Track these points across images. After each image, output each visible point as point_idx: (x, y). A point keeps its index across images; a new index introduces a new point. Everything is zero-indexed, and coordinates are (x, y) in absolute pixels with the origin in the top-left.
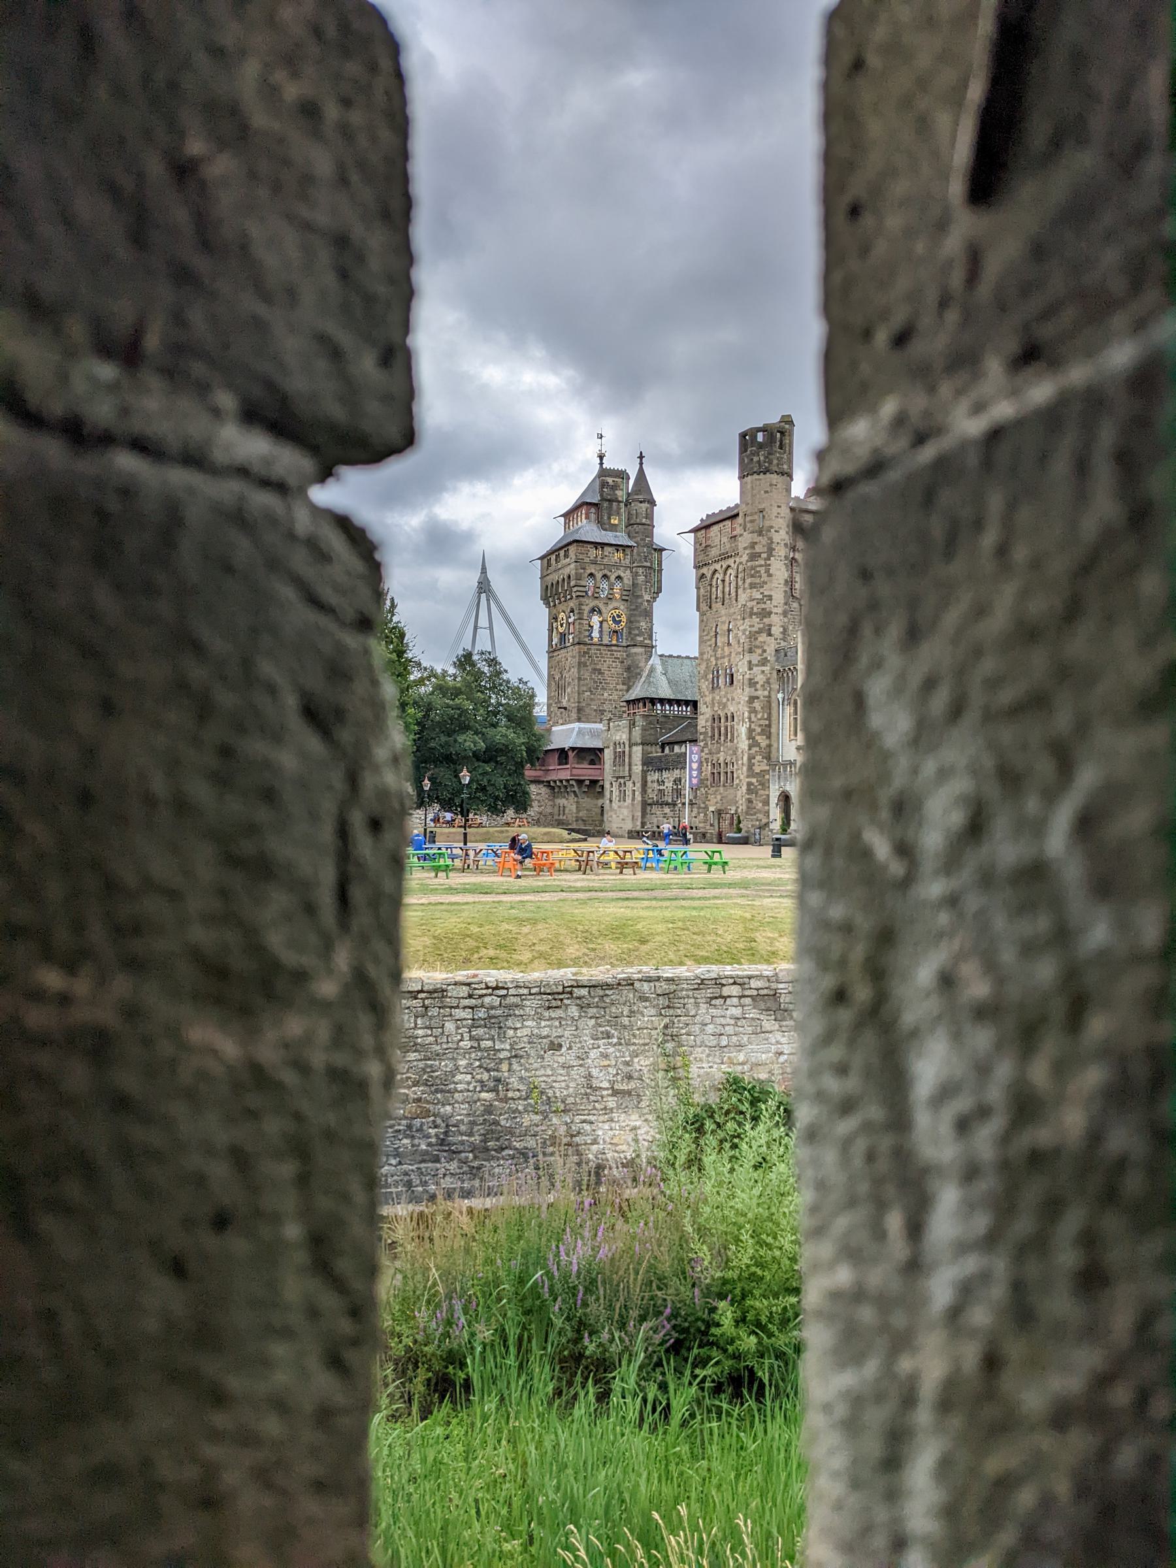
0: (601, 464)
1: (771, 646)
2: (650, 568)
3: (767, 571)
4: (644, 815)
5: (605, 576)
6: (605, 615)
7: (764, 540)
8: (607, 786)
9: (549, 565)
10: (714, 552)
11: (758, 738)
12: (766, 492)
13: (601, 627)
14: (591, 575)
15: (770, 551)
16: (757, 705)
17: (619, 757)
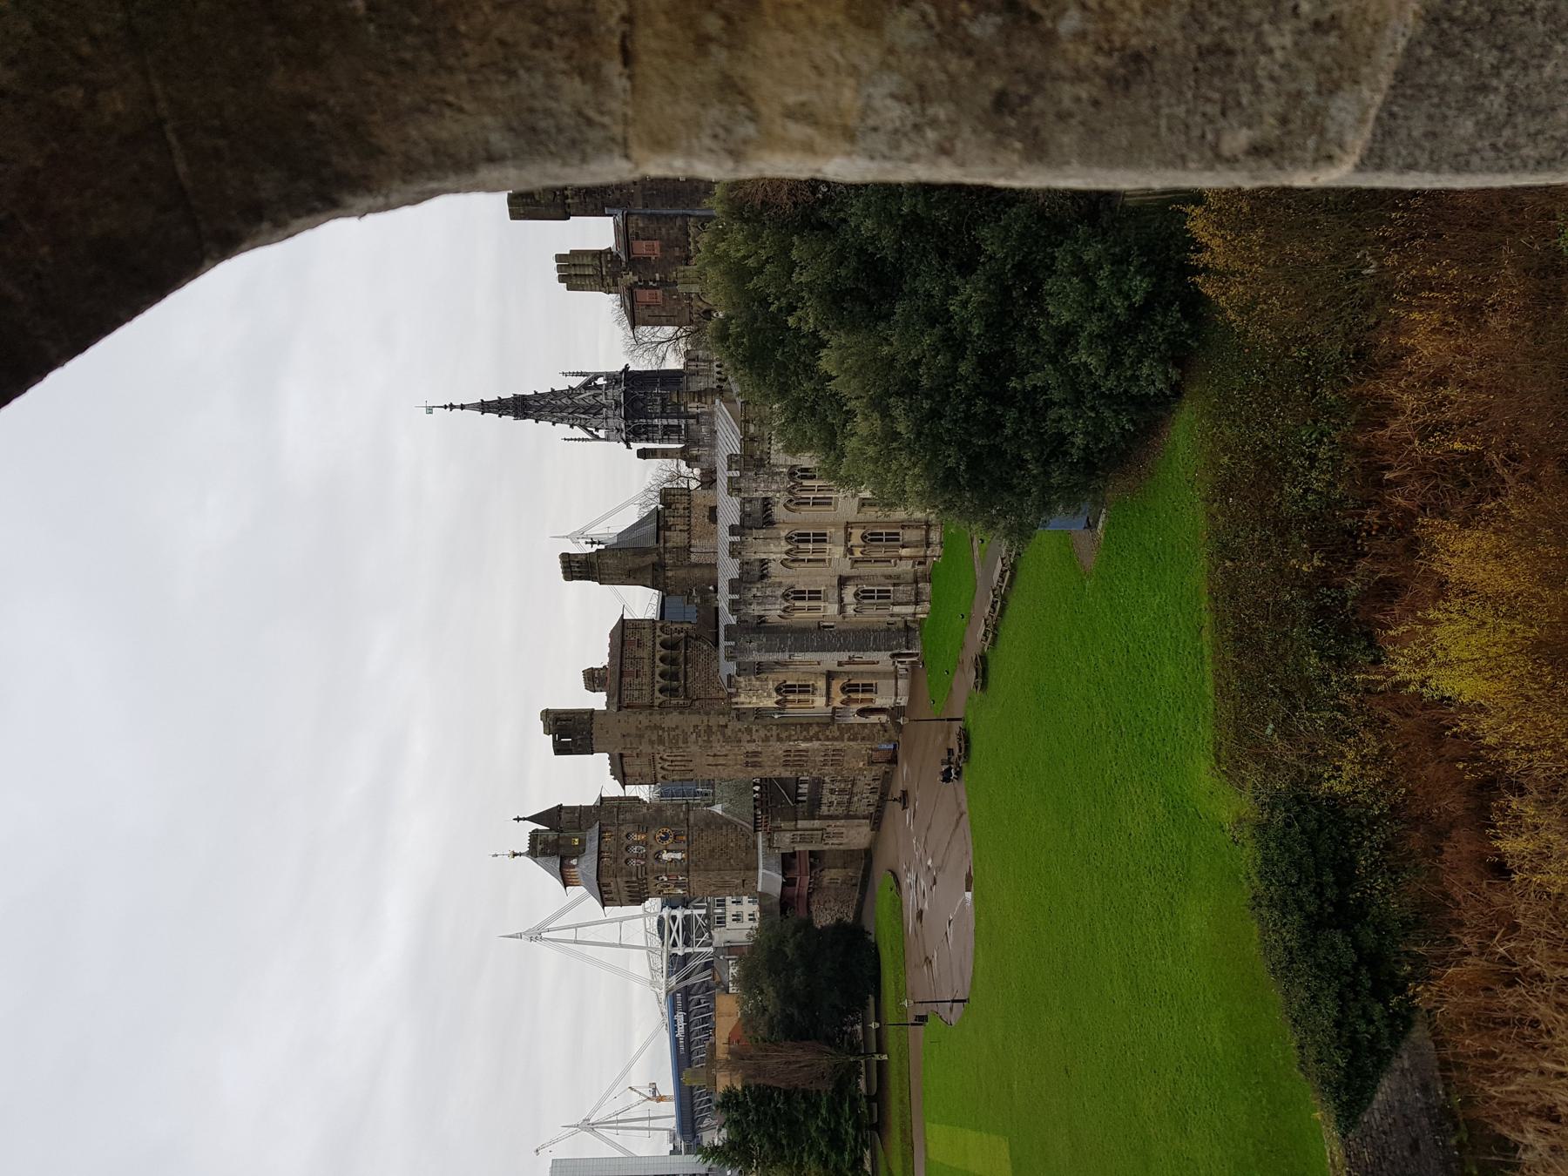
0: (520, 854)
1: (735, 725)
2: (619, 808)
3: (674, 730)
4: (855, 817)
5: (627, 849)
6: (662, 848)
7: (649, 733)
8: (826, 847)
9: (612, 899)
10: (646, 770)
11: (811, 734)
12: (607, 732)
13: (672, 851)
14: (626, 862)
15: (656, 727)
16: (784, 735)
17: (803, 840)
